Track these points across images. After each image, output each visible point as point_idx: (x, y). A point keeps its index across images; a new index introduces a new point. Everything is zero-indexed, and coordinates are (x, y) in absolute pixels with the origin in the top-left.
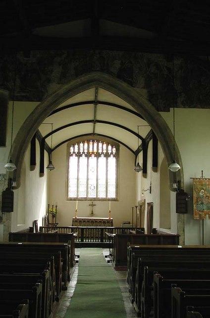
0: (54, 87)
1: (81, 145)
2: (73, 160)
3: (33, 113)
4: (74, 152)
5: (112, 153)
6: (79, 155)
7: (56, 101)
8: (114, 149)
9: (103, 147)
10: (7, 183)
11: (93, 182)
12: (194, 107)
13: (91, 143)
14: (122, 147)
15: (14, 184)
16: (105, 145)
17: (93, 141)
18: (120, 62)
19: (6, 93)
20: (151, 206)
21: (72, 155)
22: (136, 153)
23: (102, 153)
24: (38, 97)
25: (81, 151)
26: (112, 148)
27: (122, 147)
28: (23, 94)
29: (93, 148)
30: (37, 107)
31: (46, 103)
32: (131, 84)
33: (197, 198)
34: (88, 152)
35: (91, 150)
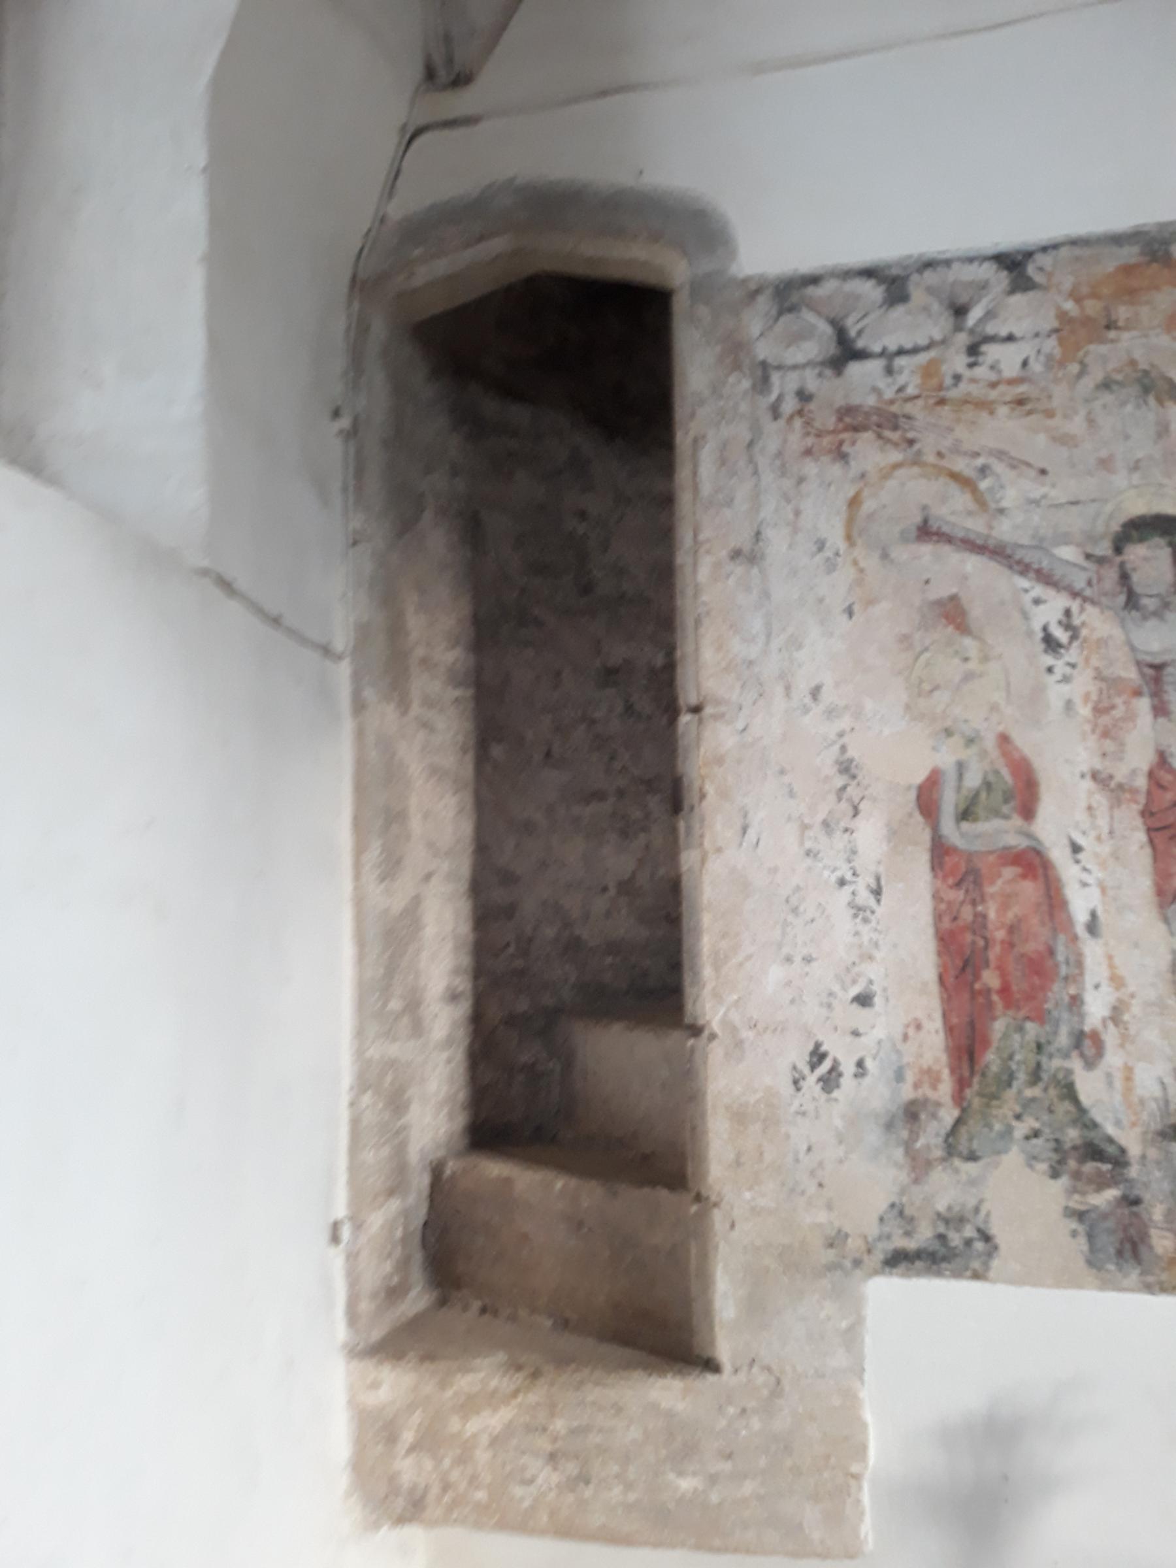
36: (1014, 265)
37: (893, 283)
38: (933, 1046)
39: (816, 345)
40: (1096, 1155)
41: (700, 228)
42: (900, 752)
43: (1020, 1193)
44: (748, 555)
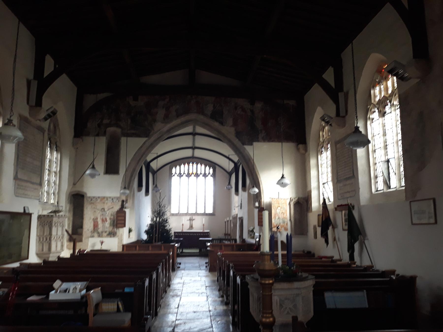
0: (160, 127)
1: (182, 166)
2: (175, 180)
3: (141, 147)
5: (209, 173)
6: (180, 175)
7: (160, 137)
8: (211, 170)
9: (201, 168)
10: (120, 203)
12: (272, 141)
13: (191, 164)
14: (217, 168)
15: (126, 205)
16: (203, 166)
17: (193, 163)
18: (213, 105)
19: (119, 130)
20: (241, 219)
21: (174, 176)
22: (230, 174)
23: (201, 174)
24: (146, 134)
25: (182, 172)
26: (210, 169)
27: (217, 168)
28: (133, 132)
30: (144, 143)
31: (153, 139)
32: (222, 123)
33: (275, 215)
34: (188, 173)
36: (99, 197)
37: (94, 197)
38: (93, 229)
39: (90, 200)
40: (98, 233)
41: (86, 194)
42: (92, 217)
43: (96, 235)
44: (87, 208)
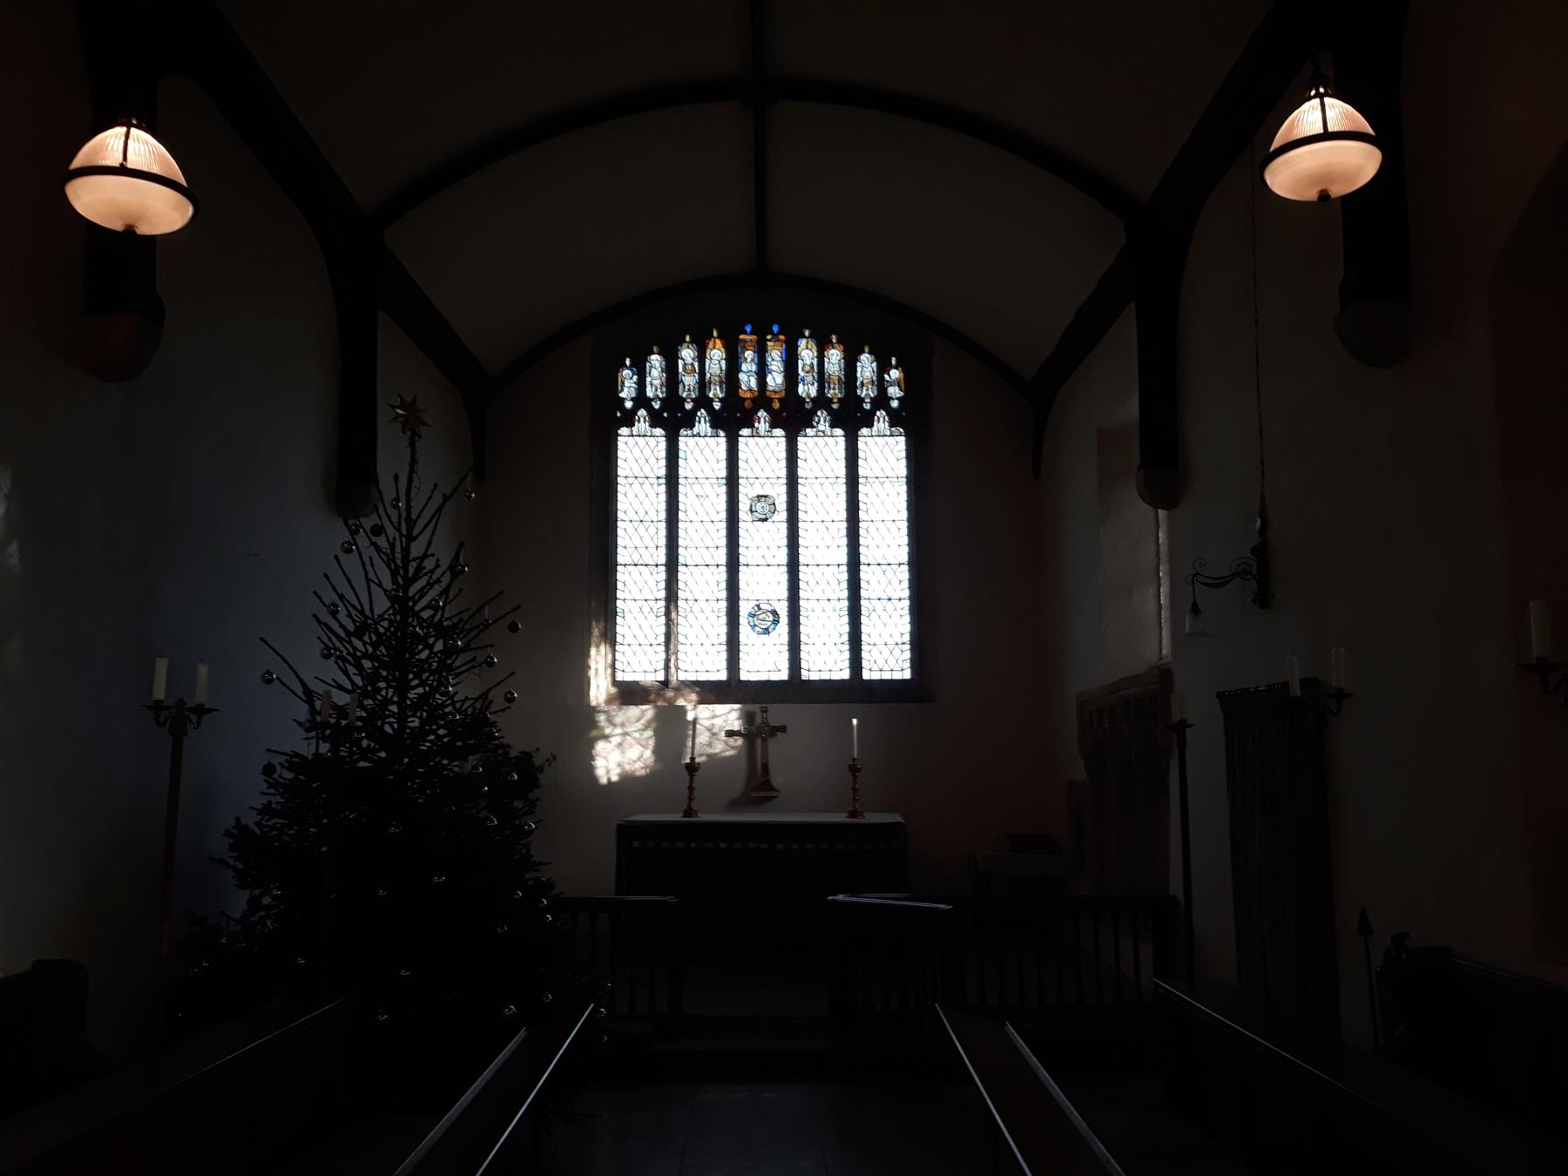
2: (638, 453)
4: (641, 400)
5: (881, 400)
6: (673, 419)
9: (818, 363)
11: (763, 584)
21: (629, 419)
23: (821, 401)
26: (883, 368)
29: (762, 372)
35: (748, 380)
